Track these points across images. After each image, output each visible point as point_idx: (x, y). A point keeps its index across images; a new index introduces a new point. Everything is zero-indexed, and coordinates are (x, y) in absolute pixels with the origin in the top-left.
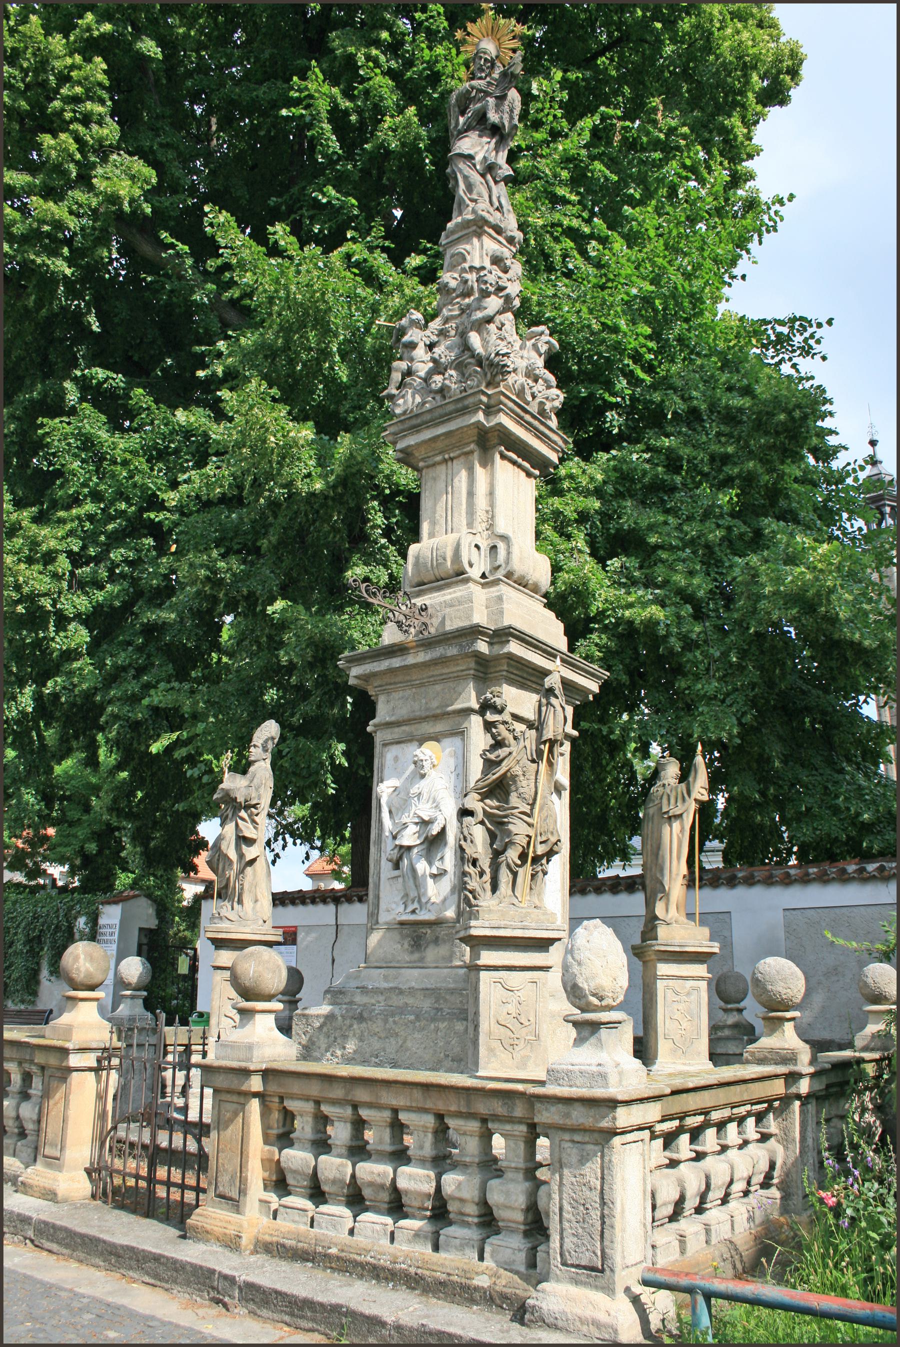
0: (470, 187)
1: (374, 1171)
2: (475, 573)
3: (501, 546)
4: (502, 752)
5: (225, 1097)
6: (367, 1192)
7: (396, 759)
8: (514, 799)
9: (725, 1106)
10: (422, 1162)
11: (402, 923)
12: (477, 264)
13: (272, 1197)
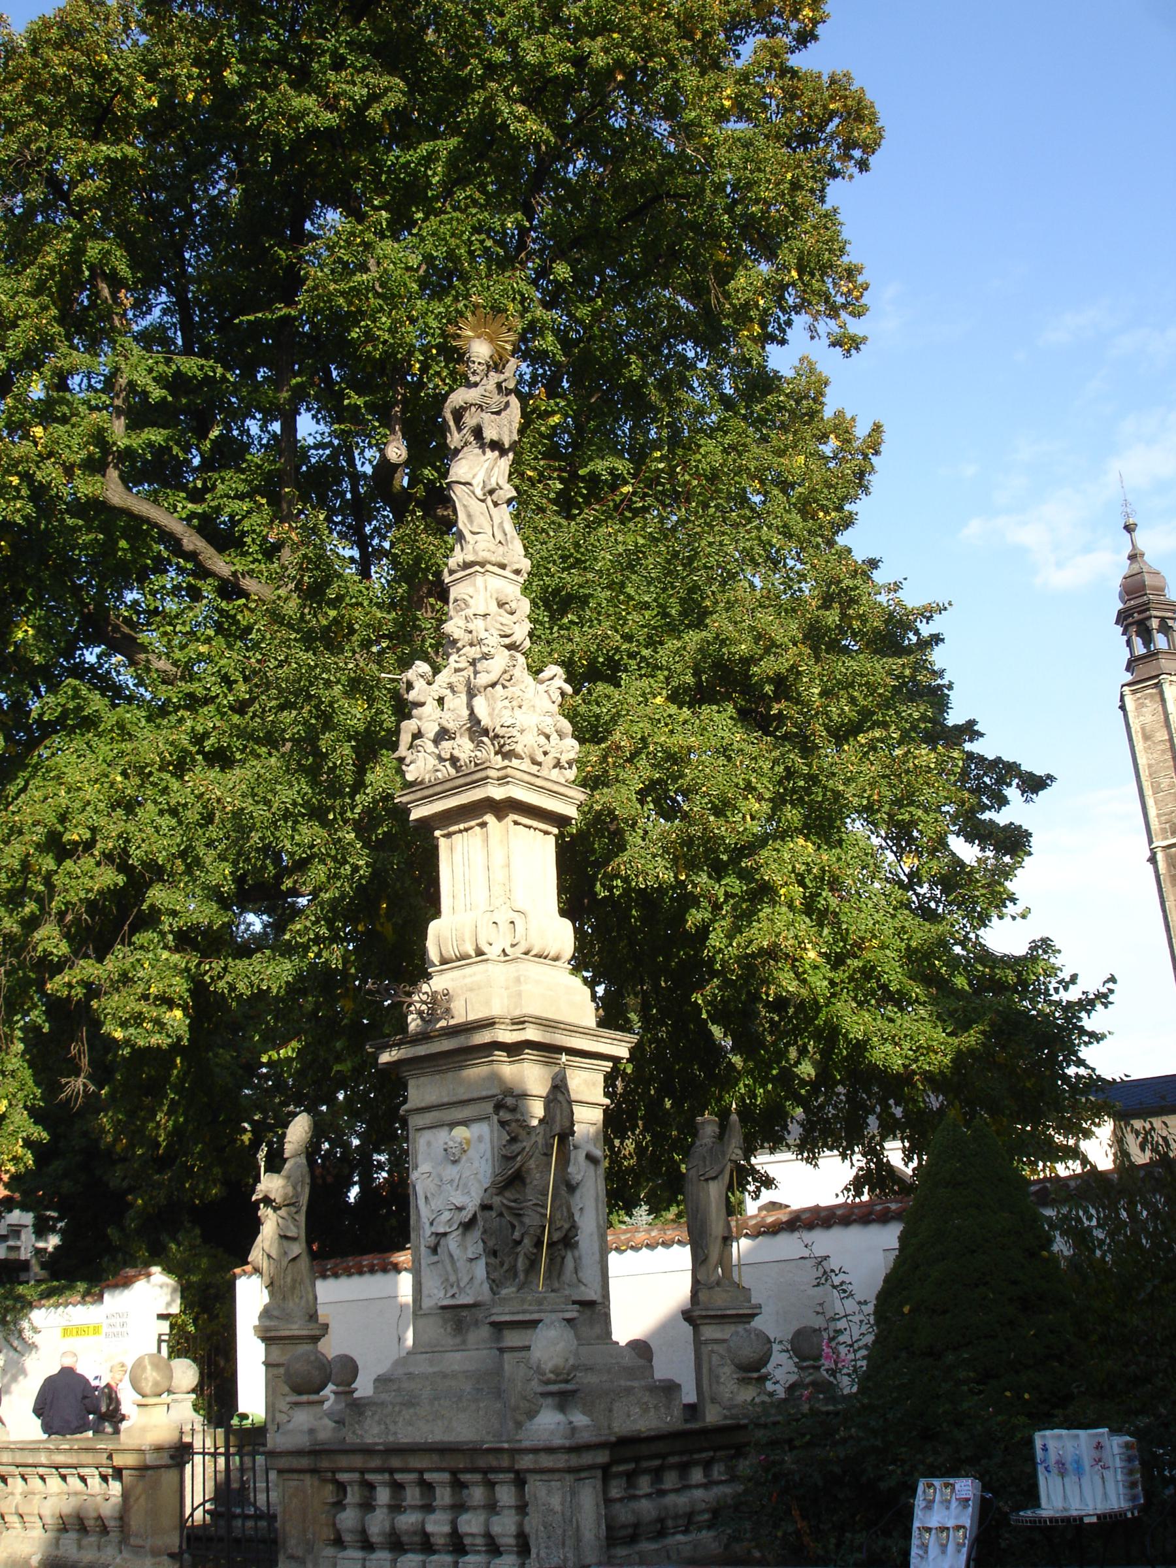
0: (469, 516)
1: (408, 1520)
2: (493, 952)
4: (516, 1147)
5: (286, 1476)
6: (405, 1539)
7: (429, 1144)
9: (681, 1453)
10: (444, 1508)
11: (444, 1308)
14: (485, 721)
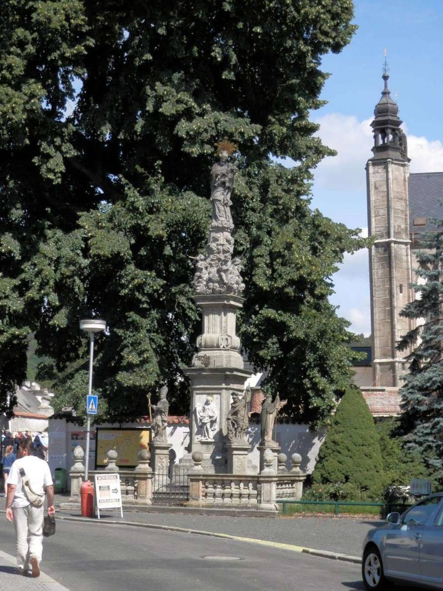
0: (219, 210)
3: (229, 338)
4: (237, 404)
8: (239, 416)
12: (222, 243)
13: (204, 498)
14: (226, 281)
